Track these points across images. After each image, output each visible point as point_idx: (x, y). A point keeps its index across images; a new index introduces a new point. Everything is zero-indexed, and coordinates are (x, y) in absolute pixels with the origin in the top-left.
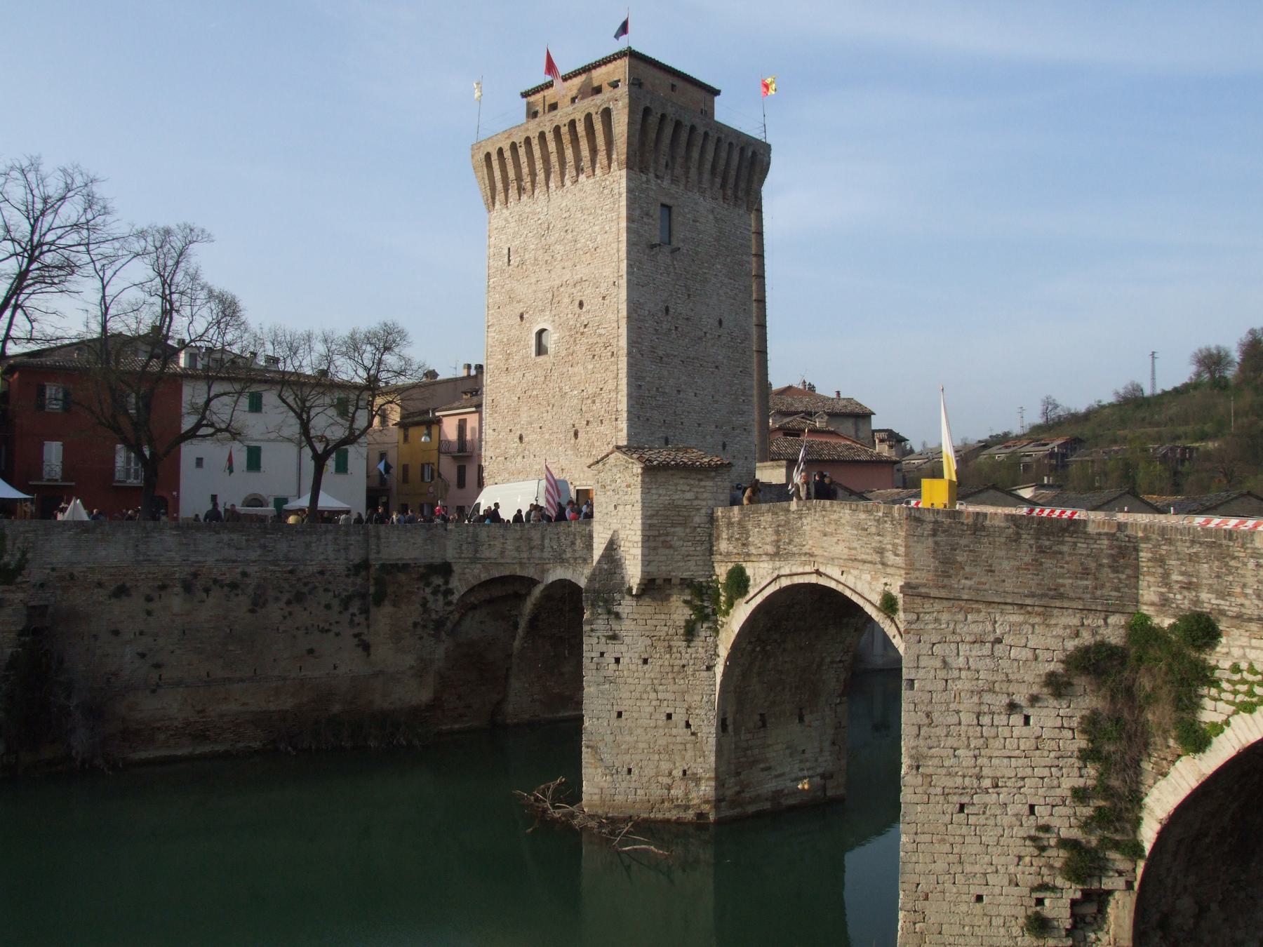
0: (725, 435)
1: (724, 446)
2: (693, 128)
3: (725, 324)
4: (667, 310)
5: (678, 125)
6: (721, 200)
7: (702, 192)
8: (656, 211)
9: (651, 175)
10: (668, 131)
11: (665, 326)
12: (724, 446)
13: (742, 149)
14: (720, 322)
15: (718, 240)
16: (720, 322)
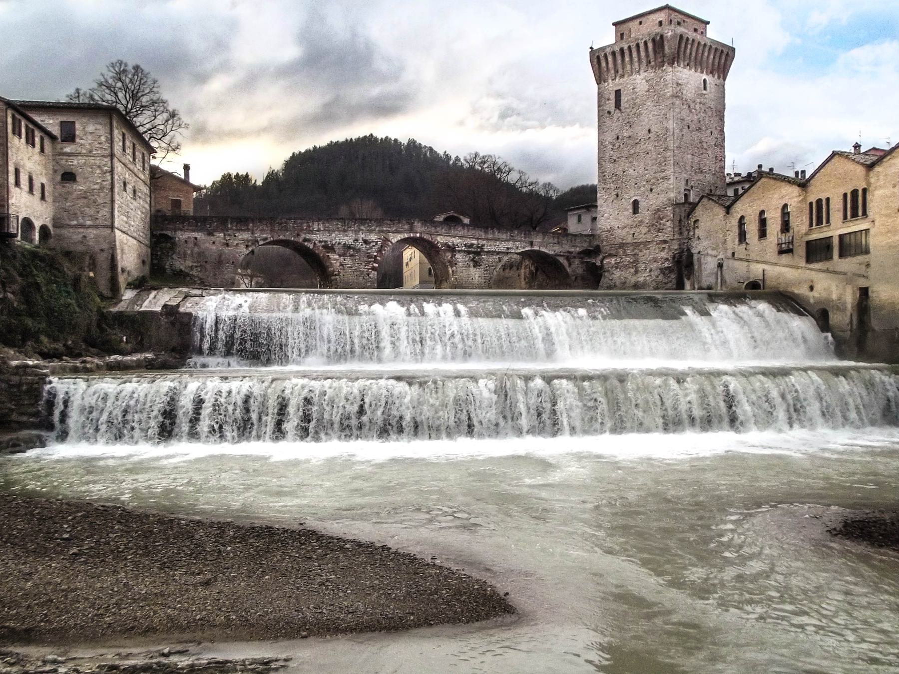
0: (653, 184)
1: (651, 190)
2: (622, 50)
3: (652, 130)
4: (618, 138)
5: (614, 53)
6: (650, 70)
7: (638, 72)
8: (613, 96)
9: (610, 81)
10: (610, 59)
11: (617, 145)
12: (651, 190)
13: (654, 40)
14: (649, 131)
15: (648, 91)
16: (649, 131)
